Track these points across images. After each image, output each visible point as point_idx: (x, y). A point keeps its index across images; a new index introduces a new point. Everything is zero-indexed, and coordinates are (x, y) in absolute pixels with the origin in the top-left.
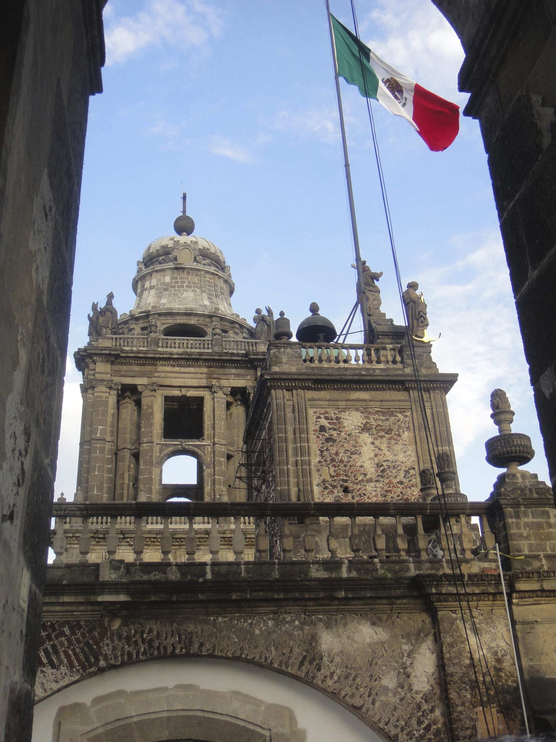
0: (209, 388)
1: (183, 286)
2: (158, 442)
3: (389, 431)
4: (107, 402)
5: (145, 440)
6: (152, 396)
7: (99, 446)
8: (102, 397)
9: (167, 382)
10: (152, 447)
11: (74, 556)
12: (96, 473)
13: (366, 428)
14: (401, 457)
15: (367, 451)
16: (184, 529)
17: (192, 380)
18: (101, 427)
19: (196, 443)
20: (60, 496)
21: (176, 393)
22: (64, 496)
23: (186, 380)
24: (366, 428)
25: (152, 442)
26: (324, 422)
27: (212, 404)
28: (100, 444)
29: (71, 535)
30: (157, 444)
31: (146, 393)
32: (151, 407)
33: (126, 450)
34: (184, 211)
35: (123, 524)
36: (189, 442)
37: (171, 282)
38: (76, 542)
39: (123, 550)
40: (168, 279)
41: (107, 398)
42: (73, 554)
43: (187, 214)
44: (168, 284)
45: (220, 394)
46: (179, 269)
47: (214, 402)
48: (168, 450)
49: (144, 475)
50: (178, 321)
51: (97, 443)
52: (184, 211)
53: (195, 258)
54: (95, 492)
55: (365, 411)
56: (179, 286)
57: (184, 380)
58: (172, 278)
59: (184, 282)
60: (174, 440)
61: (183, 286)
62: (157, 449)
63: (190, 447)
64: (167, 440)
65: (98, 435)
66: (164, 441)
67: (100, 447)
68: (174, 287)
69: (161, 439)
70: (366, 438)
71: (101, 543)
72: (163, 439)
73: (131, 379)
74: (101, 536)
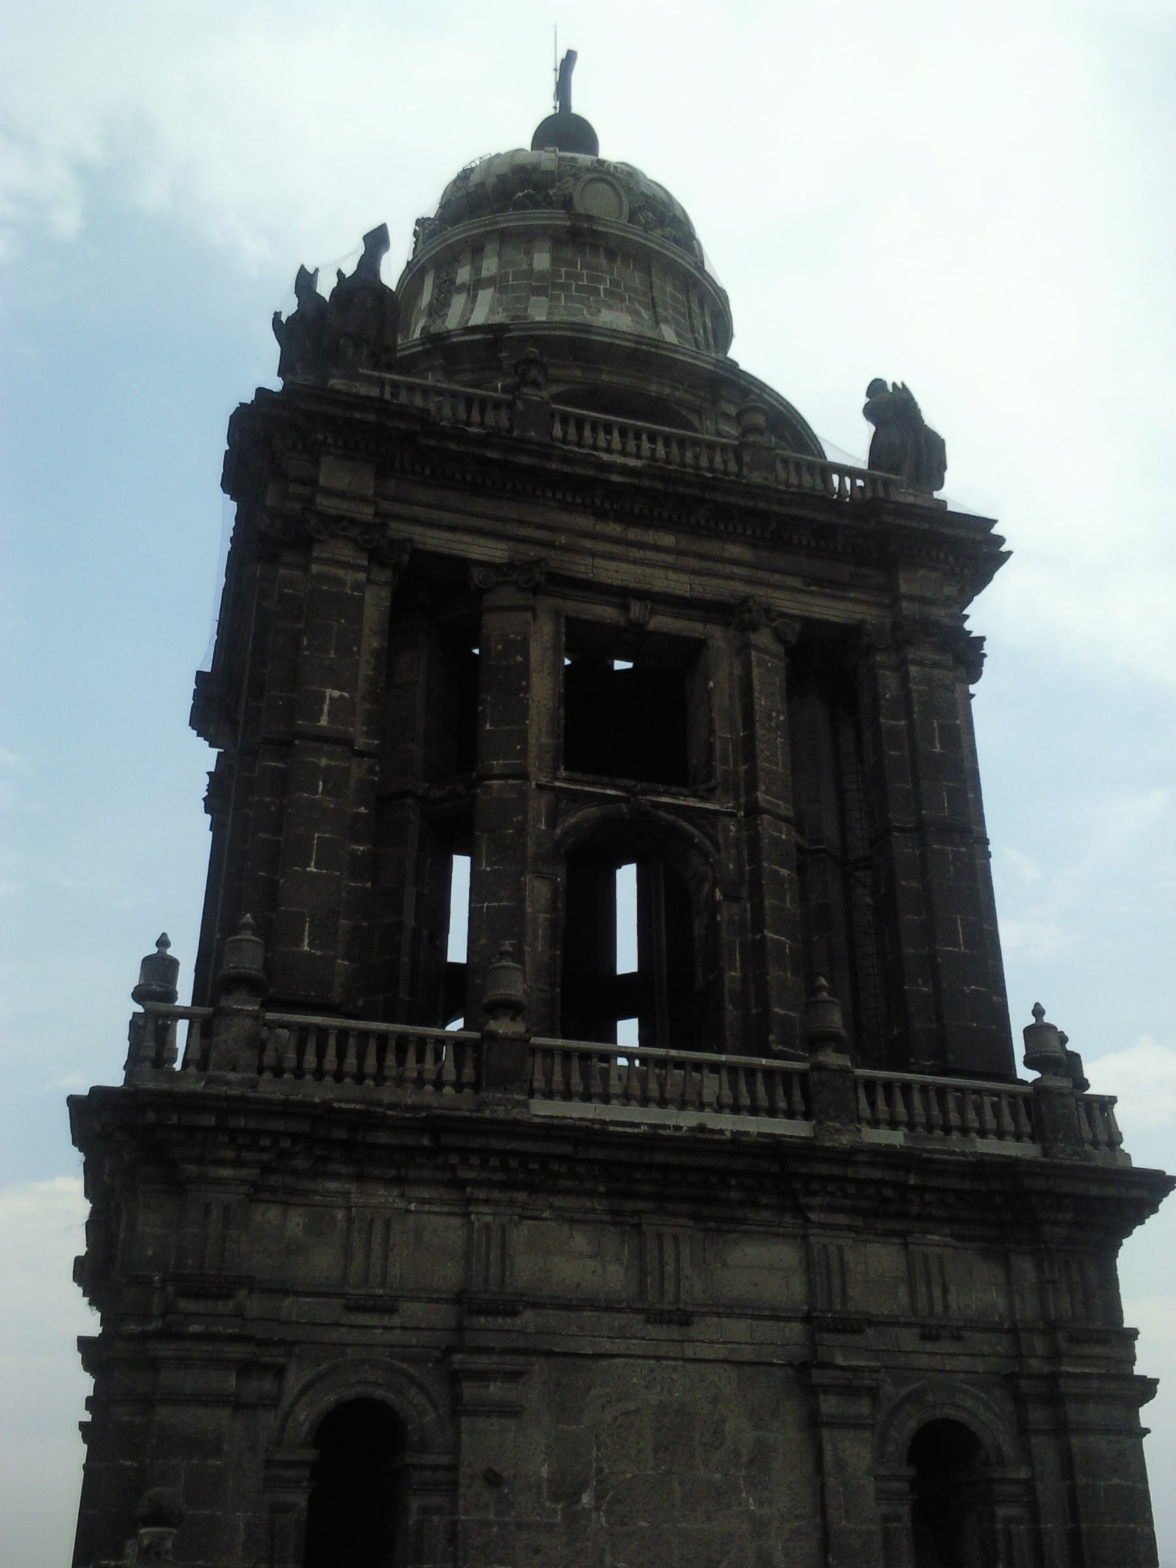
1: (596, 292)
2: (543, 780)
4: (359, 604)
5: (497, 764)
6: (525, 608)
7: (324, 762)
8: (341, 582)
9: (582, 567)
16: (678, 1128)
17: (671, 575)
19: (681, 801)
20: (155, 950)
22: (170, 952)
23: (649, 571)
25: (525, 776)
27: (738, 670)
29: (210, 1120)
30: (540, 787)
32: (523, 646)
33: (409, 801)
35: (429, 1088)
37: (555, 274)
38: (230, 1154)
39: (422, 1201)
40: (542, 261)
41: (358, 586)
42: (207, 1208)
43: (578, 107)
44: (542, 275)
45: (763, 638)
47: (747, 665)
48: (579, 814)
54: (306, 948)
57: (639, 570)
58: (554, 261)
59: (600, 280)
60: (606, 779)
62: (539, 805)
63: (662, 814)
64: (578, 776)
65: (324, 721)
66: (565, 780)
67: (327, 767)
68: (565, 288)
69: (555, 769)
71: (332, 1167)
73: (447, 535)
74: (340, 1134)
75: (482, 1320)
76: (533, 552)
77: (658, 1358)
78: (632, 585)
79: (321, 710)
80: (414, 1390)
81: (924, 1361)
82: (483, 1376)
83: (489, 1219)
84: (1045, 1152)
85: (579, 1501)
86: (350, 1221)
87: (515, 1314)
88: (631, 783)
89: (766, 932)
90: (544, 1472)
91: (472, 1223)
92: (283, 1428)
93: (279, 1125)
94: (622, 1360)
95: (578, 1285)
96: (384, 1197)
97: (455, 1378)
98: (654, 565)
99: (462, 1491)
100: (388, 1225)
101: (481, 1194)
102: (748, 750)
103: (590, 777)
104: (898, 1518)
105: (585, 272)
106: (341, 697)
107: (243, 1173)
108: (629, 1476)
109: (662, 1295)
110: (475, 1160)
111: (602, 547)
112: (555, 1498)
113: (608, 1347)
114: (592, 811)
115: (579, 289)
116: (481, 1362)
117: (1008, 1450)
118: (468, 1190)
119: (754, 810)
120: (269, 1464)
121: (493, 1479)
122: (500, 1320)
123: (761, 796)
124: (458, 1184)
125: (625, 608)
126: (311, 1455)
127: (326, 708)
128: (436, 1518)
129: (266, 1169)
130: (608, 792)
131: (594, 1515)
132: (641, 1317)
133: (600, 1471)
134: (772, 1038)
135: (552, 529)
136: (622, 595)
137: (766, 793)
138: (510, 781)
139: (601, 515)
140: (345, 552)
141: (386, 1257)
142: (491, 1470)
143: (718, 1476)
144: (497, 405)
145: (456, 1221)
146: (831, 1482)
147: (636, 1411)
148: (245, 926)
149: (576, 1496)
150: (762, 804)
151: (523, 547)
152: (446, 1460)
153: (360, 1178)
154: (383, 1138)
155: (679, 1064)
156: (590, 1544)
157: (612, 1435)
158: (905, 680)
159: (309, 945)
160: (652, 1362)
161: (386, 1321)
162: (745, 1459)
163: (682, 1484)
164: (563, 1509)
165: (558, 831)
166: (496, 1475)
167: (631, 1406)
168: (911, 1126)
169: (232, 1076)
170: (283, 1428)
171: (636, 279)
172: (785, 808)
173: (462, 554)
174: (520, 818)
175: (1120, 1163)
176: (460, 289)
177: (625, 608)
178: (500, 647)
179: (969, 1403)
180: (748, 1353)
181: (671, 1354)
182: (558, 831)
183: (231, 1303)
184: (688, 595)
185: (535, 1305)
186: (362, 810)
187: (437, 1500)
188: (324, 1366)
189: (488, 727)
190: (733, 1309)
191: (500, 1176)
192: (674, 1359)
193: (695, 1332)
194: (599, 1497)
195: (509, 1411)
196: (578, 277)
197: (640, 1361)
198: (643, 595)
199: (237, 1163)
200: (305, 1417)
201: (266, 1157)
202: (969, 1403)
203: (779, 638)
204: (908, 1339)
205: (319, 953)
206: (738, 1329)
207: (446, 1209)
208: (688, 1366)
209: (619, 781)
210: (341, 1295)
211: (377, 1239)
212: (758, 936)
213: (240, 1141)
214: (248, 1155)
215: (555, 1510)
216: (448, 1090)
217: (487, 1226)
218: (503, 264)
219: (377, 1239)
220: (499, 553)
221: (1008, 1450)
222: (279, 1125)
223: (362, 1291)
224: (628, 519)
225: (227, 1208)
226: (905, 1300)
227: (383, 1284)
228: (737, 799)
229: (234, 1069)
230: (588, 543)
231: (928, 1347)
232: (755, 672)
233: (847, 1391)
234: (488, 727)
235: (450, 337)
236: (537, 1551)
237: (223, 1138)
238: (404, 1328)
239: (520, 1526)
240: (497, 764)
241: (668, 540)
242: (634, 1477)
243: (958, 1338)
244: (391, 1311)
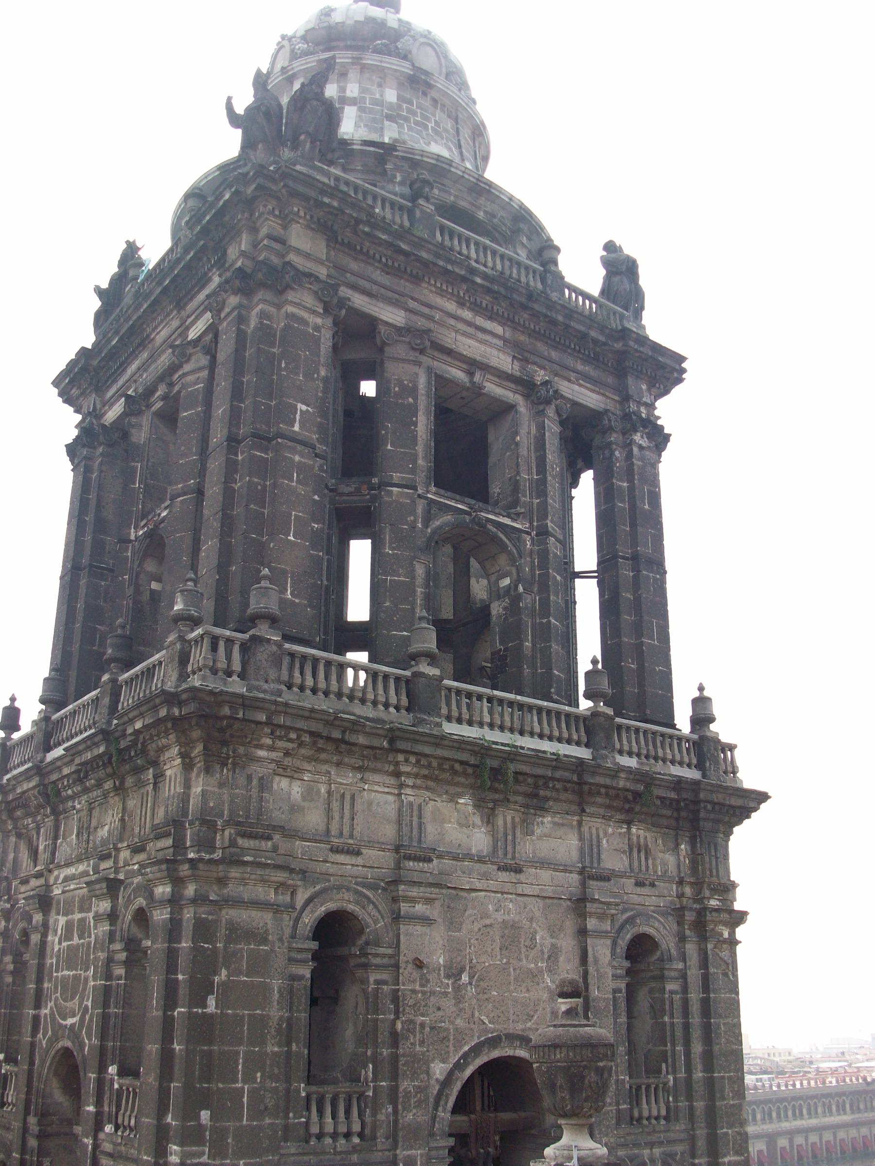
0: (527, 386)
1: (426, 127)
5: (396, 476)
7: (297, 458)
9: (448, 339)
10: (413, 502)
11: (255, 782)
12: (291, 538)
18: (304, 408)
19: (501, 519)
25: (415, 488)
27: (534, 430)
28: (302, 456)
31: (399, 350)
35: (381, 707)
36: (488, 512)
37: (400, 107)
38: (269, 741)
40: (391, 96)
41: (317, 328)
42: (249, 778)
44: (391, 106)
48: (441, 520)
49: (395, 573)
51: (294, 451)
56: (417, 123)
57: (483, 348)
58: (399, 98)
59: (428, 119)
60: (458, 497)
63: (490, 527)
64: (442, 492)
65: (296, 428)
66: (435, 494)
68: (406, 119)
71: (323, 756)
72: (434, 489)
75: (411, 864)
76: (421, 323)
77: (502, 893)
78: (478, 358)
79: (295, 418)
80: (371, 907)
81: (636, 899)
82: (413, 900)
83: (411, 799)
84: (704, 776)
85: (460, 979)
86: (329, 793)
87: (430, 860)
88: (473, 502)
89: (551, 618)
90: (441, 961)
91: (403, 801)
92: (295, 927)
93: (301, 724)
94: (483, 893)
95: (460, 845)
96: (349, 778)
97: (395, 900)
98: (491, 345)
99: (401, 971)
100: (353, 798)
101: (410, 782)
103: (449, 494)
104: (620, 991)
105: (419, 111)
106: (307, 410)
107: (274, 755)
108: (487, 964)
109: (506, 854)
110: (413, 759)
111: (460, 326)
112: (448, 977)
113: (478, 885)
114: (448, 518)
115: (417, 123)
116: (414, 892)
117: (674, 952)
118: (403, 778)
120: (290, 949)
121: (419, 964)
122: (421, 864)
124: (397, 774)
125: (471, 374)
126: (314, 945)
127: (298, 417)
128: (385, 987)
129: (287, 754)
130: (460, 506)
131: (469, 988)
132: (495, 867)
133: (471, 961)
134: (553, 690)
136: (472, 365)
137: (552, 521)
138: (406, 490)
139: (461, 304)
140: (309, 300)
141: (353, 819)
142: (417, 958)
143: (533, 965)
144: (401, 208)
145: (391, 798)
146: (591, 969)
147: (491, 925)
148: (265, 577)
149: (458, 976)
150: (550, 529)
151: (414, 318)
152: (390, 951)
153: (338, 764)
154: (361, 740)
155: (521, 706)
156: (467, 1004)
157: (477, 939)
158: (630, 456)
159: (291, 594)
160: (499, 895)
161: (354, 860)
162: (546, 956)
163: (514, 969)
164: (453, 983)
165: (429, 530)
166: (421, 962)
167: (488, 922)
168: (638, 755)
169: (266, 686)
170: (295, 927)
173: (376, 314)
174: (412, 518)
175: (738, 785)
177: (471, 374)
178: (397, 389)
179: (657, 924)
180: (549, 891)
181: (511, 891)
182: (429, 530)
183: (270, 843)
184: (510, 372)
185: (440, 857)
186: (316, 497)
187: (384, 976)
188: (318, 887)
189: (389, 447)
190: (543, 864)
191: (425, 772)
192: (511, 894)
193: (522, 877)
194: (471, 977)
195: (427, 921)
196: (414, 114)
197: (493, 895)
198: (485, 368)
199: (272, 748)
200: (309, 919)
201: (290, 745)
202: (657, 924)
203: (558, 412)
204: (629, 883)
205: (297, 601)
206: (545, 875)
207: (386, 790)
208: (519, 898)
209: (467, 500)
210: (328, 842)
211: (347, 807)
212: (545, 621)
213: (278, 733)
214: (280, 744)
215: (448, 984)
216: (392, 710)
217: (411, 804)
218: (363, 90)
219: (347, 807)
220: (399, 319)
221: (674, 952)
222: (301, 724)
223: (342, 840)
224: (476, 308)
225: (261, 779)
226: (627, 863)
227: (351, 836)
228: (531, 523)
229: (266, 682)
230: (452, 322)
231: (639, 890)
233: (601, 917)
234: (389, 447)
235: (353, 144)
236: (439, 1009)
237: (267, 730)
238: (364, 866)
239: (433, 993)
240: (396, 476)
242: (490, 965)
243: (653, 885)
244: (358, 853)
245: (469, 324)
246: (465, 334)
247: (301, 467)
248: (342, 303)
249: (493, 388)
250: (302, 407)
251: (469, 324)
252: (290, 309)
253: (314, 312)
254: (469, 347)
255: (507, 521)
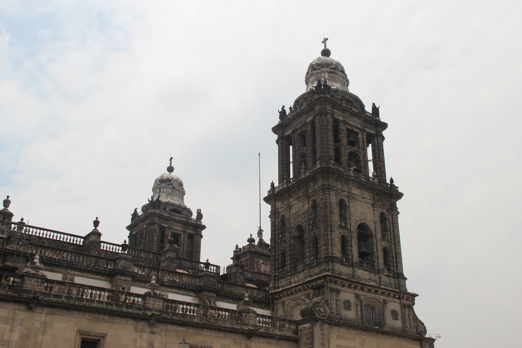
0: (183, 231)
1: (174, 194)
3: (266, 264)
9: (173, 227)
13: (263, 263)
14: (267, 269)
15: (263, 267)
21: (174, 231)
24: (263, 263)
26: (257, 261)
31: (167, 229)
34: (171, 164)
37: (171, 192)
40: (170, 191)
46: (173, 188)
47: (184, 236)
50: (176, 208)
52: (171, 164)
53: (178, 185)
55: (263, 260)
56: (173, 194)
58: (171, 191)
61: (174, 194)
68: (172, 194)
70: (263, 265)
102: (184, 244)
115: (173, 194)
119: (184, 249)
123: (184, 248)
135: (171, 224)
136: (176, 230)
139: (175, 223)
140: (156, 226)
158: (196, 238)
171: (178, 193)
172: (186, 249)
176: (162, 192)
196: (173, 193)
203: (187, 234)
218: (166, 190)
224: (177, 223)
232: (185, 237)
241: (180, 225)
245: (176, 225)
246: (175, 226)
247: (155, 244)
248: (160, 225)
249: (179, 232)
250: (155, 238)
251: (176, 225)
252: (155, 227)
253: (157, 227)
254: (176, 228)
255: (179, 248)
